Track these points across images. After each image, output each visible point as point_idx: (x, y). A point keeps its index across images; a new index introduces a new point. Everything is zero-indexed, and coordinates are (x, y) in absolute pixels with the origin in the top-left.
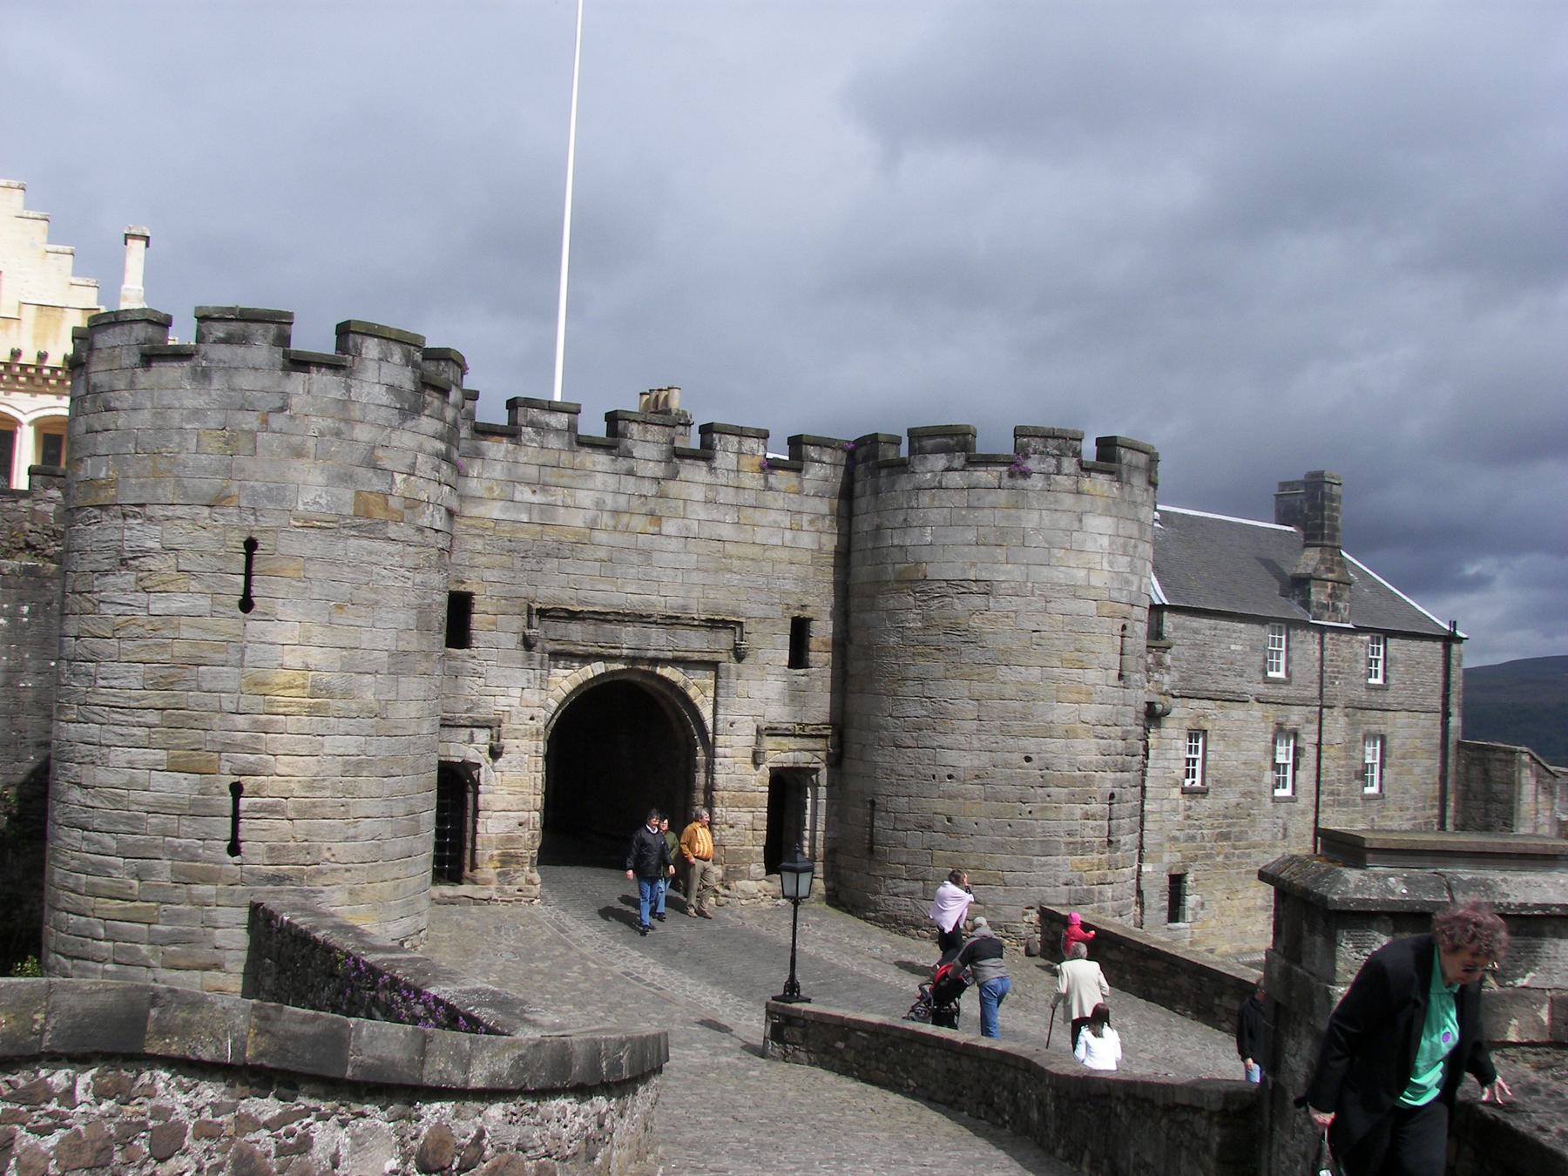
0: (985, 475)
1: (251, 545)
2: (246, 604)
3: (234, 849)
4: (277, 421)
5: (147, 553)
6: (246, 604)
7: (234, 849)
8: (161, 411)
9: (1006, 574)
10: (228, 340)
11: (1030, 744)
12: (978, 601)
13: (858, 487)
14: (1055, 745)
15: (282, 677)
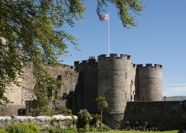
0: (153, 68)
1: (126, 73)
2: (126, 78)
3: (126, 98)
4: (127, 63)
5: (119, 74)
6: (126, 78)
7: (126, 98)
8: (119, 62)
9: (155, 77)
10: (124, 57)
11: (158, 92)
12: (153, 79)
13: (139, 69)
14: (159, 92)
15: (128, 84)
